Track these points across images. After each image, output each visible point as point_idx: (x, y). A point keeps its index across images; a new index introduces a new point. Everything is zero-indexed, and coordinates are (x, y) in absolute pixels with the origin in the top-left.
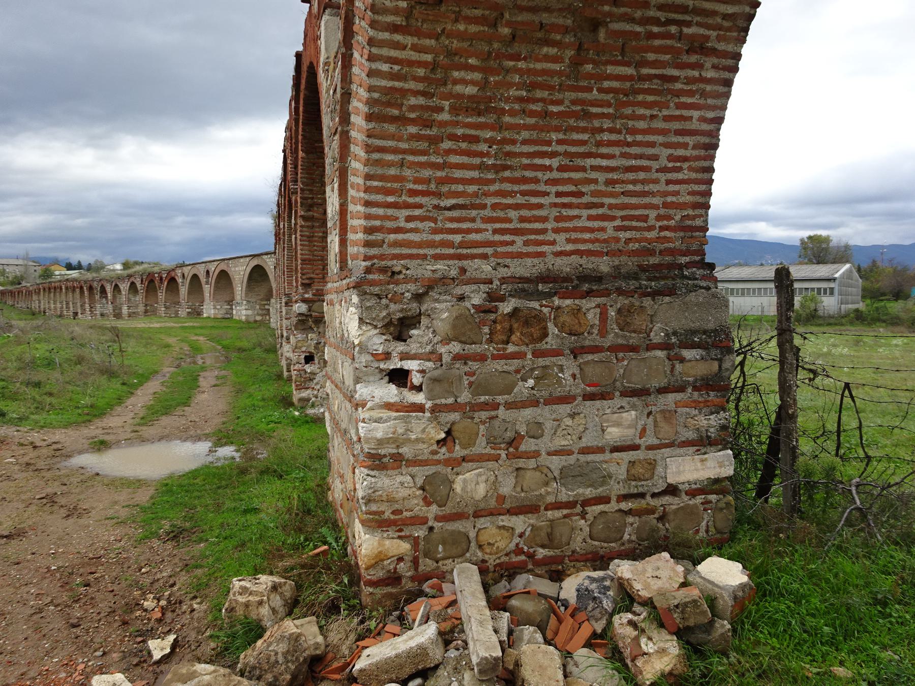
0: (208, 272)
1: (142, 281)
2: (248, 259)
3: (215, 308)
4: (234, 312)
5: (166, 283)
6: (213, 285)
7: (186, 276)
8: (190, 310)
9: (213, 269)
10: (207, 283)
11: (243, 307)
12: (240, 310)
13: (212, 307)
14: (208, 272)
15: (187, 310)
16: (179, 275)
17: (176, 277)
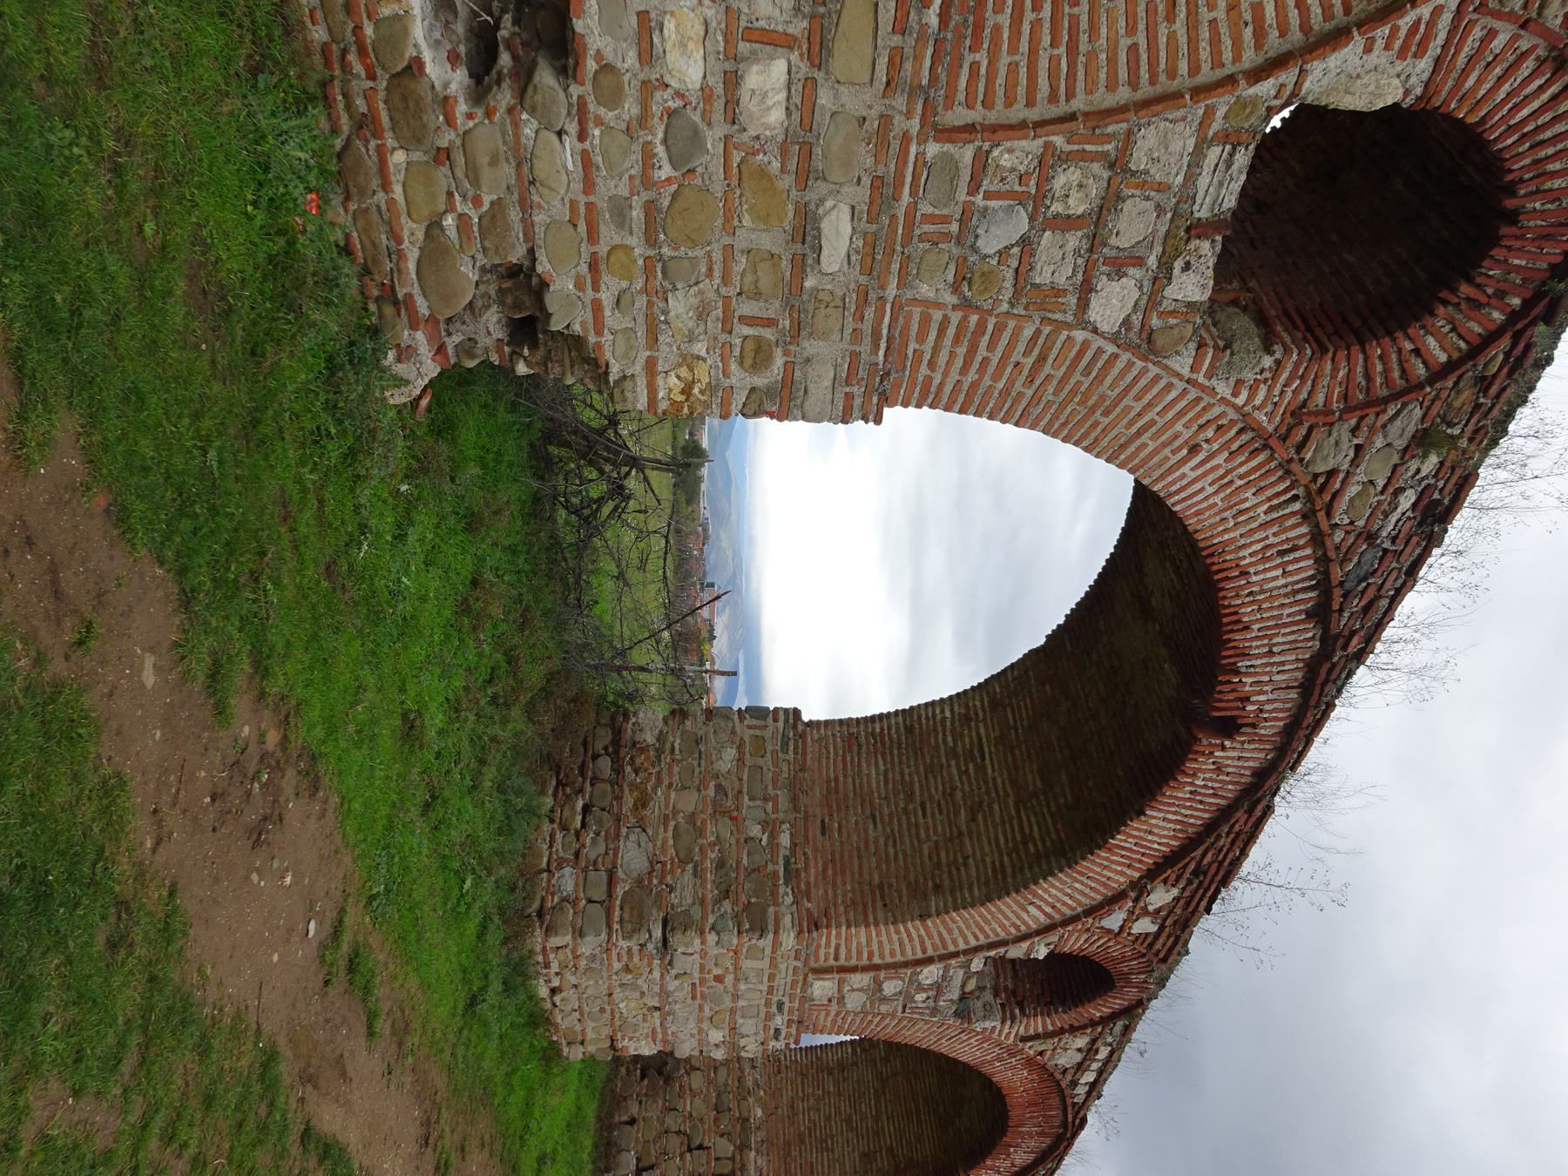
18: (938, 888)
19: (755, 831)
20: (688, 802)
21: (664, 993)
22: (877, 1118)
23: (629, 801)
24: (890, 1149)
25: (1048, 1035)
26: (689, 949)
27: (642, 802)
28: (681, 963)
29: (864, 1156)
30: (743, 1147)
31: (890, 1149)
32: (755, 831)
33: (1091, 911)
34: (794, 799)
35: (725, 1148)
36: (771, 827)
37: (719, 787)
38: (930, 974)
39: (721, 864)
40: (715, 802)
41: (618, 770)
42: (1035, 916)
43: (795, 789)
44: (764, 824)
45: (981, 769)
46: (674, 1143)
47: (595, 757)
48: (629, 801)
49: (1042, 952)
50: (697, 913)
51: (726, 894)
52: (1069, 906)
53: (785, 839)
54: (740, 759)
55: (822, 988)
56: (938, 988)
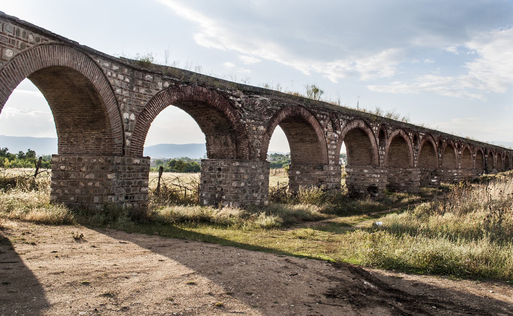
18: (407, 155)
19: (400, 172)
20: (397, 179)
21: (415, 182)
22: (425, 153)
23: (396, 185)
24: (429, 152)
25: (419, 140)
26: (413, 179)
27: (397, 184)
28: (413, 180)
29: (429, 155)
30: (428, 171)
31: (429, 152)
32: (400, 172)
33: (410, 140)
34: (397, 168)
35: (428, 173)
36: (400, 170)
37: (395, 176)
38: (415, 155)
39: (404, 176)
40: (397, 176)
41: (393, 186)
42: (410, 146)
43: (395, 167)
44: (399, 171)
45: (395, 149)
46: (427, 180)
47: (391, 189)
48: (396, 185)
49: (413, 144)
50: (409, 178)
51: (407, 175)
52: (410, 142)
53: (401, 169)
54: (392, 173)
55: (415, 166)
56: (416, 153)
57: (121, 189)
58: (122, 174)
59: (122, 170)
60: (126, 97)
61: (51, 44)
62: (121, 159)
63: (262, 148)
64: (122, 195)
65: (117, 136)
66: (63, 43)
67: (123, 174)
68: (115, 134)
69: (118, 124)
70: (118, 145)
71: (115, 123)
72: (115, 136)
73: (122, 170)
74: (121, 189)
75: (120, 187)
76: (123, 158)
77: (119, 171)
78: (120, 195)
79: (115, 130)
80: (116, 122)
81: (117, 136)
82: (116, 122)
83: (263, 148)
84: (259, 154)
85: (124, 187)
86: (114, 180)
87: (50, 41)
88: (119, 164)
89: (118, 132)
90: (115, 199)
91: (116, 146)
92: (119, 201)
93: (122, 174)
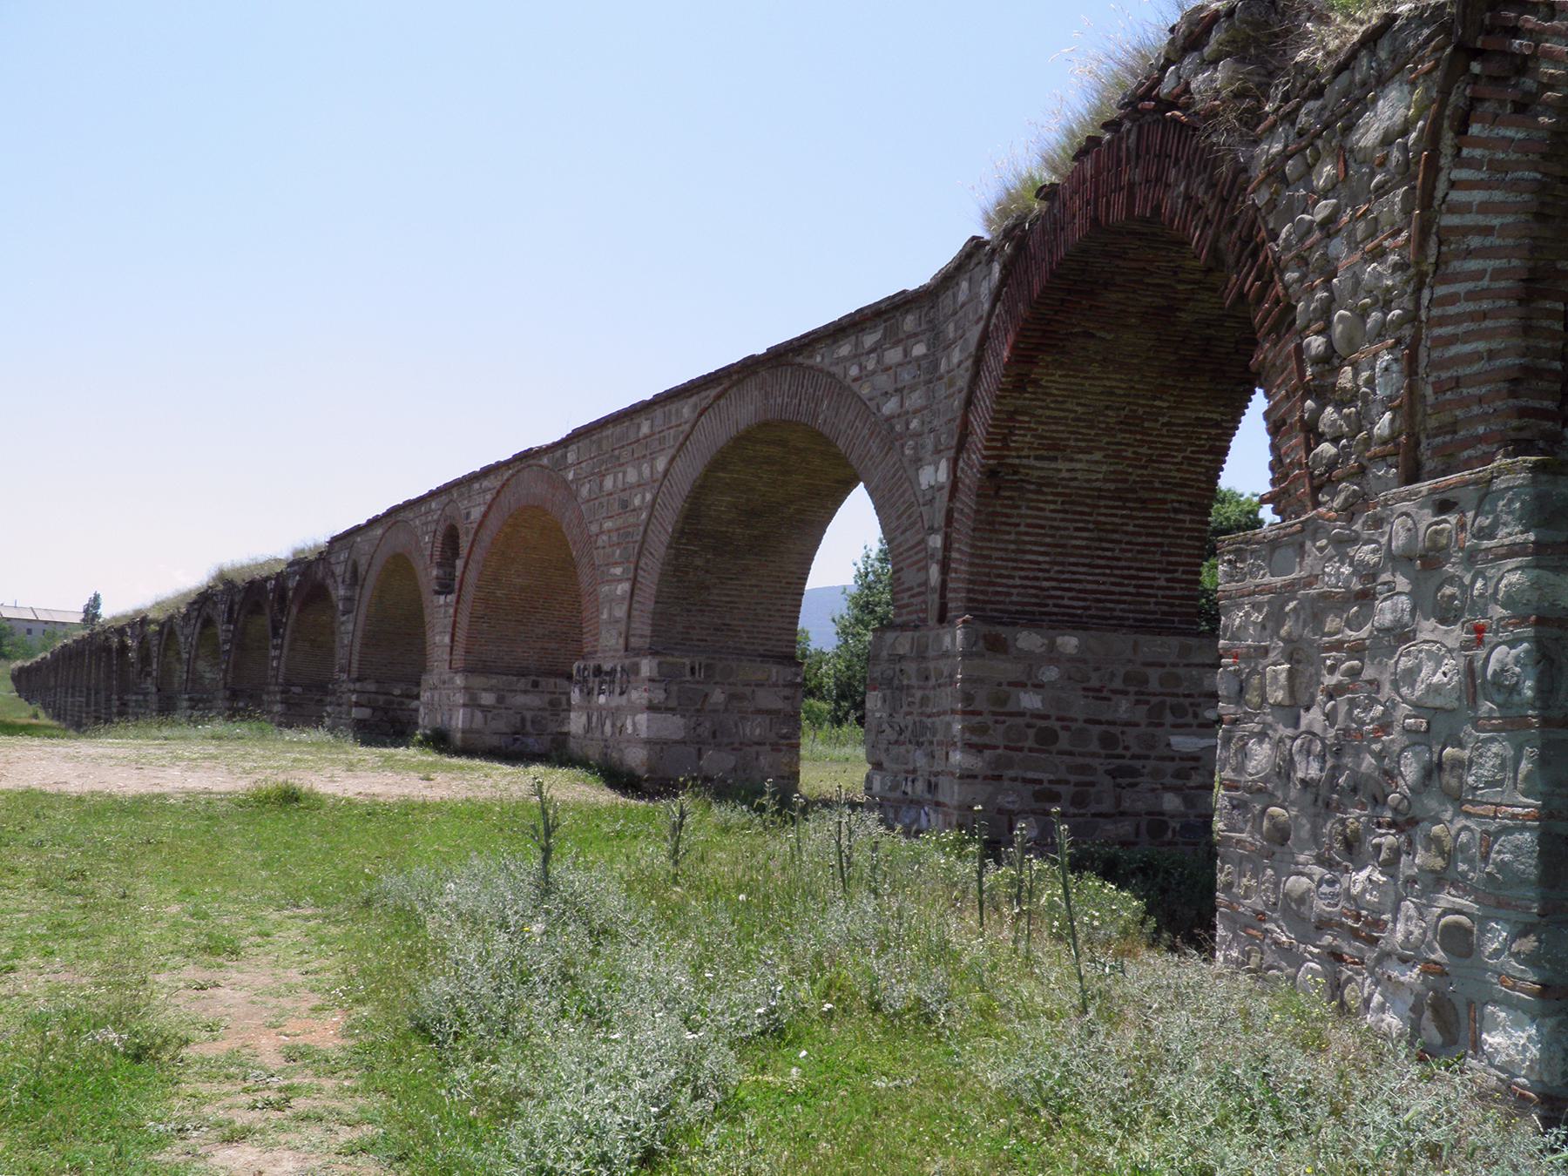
0: (451, 538)
1: (231, 610)
2: (687, 410)
3: (472, 704)
4: (576, 723)
5: (294, 610)
6: (470, 592)
7: (362, 569)
8: (364, 713)
9: (476, 513)
10: (445, 587)
11: (638, 696)
12: (615, 712)
13: (460, 699)
14: (451, 538)
15: (356, 713)
16: (339, 570)
17: (329, 581)
57: (908, 752)
58: (913, 696)
59: (914, 682)
60: (915, 412)
61: (718, 397)
62: (909, 640)
63: (1442, 321)
64: (914, 771)
65: (908, 561)
66: (735, 377)
67: (919, 694)
68: (901, 554)
69: (910, 517)
70: (916, 590)
71: (899, 517)
72: (904, 560)
73: (914, 682)
74: (908, 752)
75: (904, 743)
76: (917, 634)
77: (905, 682)
78: (907, 772)
79: (902, 538)
80: (902, 514)
81: (908, 561)
82: (902, 514)
83: (1457, 319)
84: (1388, 403)
85: (922, 744)
86: (878, 715)
87: (713, 393)
88: (902, 658)
89: (912, 543)
90: (883, 783)
91: (906, 595)
92: (897, 794)
93: (913, 696)
